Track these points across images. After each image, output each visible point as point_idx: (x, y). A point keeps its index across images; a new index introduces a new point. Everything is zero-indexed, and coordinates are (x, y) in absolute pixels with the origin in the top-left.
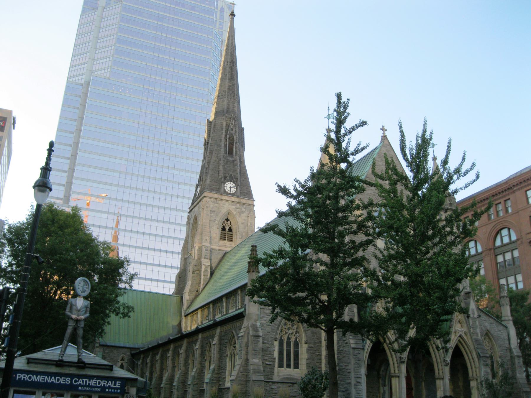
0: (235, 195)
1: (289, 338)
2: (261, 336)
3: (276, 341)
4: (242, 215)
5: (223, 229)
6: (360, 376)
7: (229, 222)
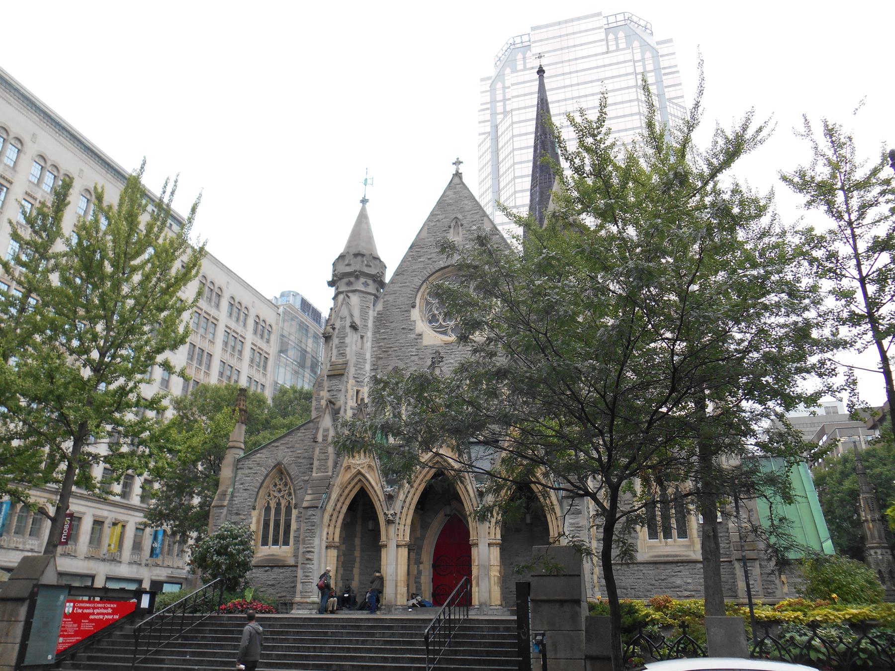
1: (279, 504)
2: (224, 506)
3: (254, 509)
6: (312, 550)
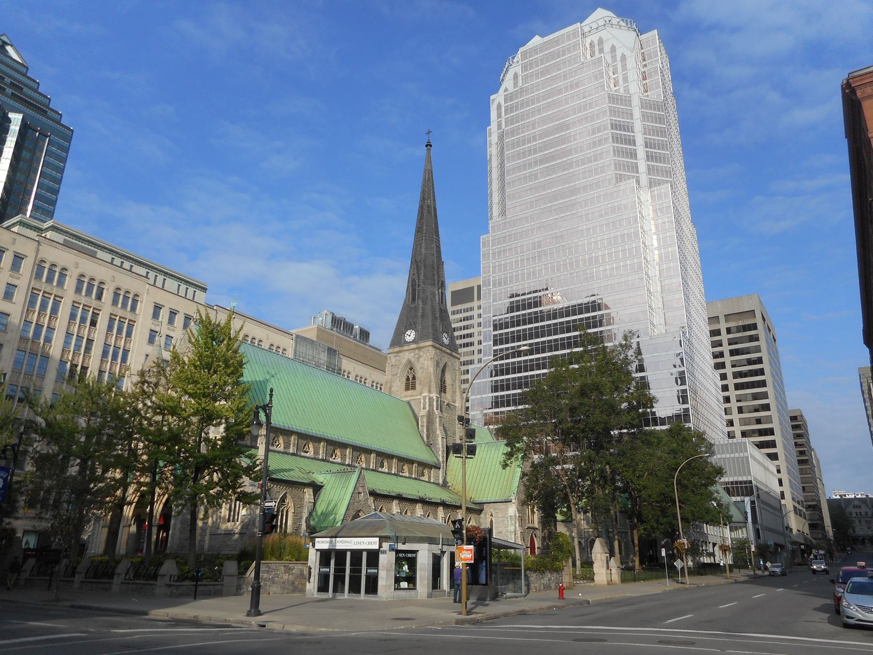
0: (414, 342)
4: (420, 359)
5: (408, 379)
7: (412, 370)
